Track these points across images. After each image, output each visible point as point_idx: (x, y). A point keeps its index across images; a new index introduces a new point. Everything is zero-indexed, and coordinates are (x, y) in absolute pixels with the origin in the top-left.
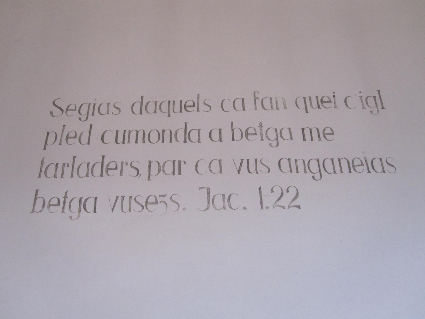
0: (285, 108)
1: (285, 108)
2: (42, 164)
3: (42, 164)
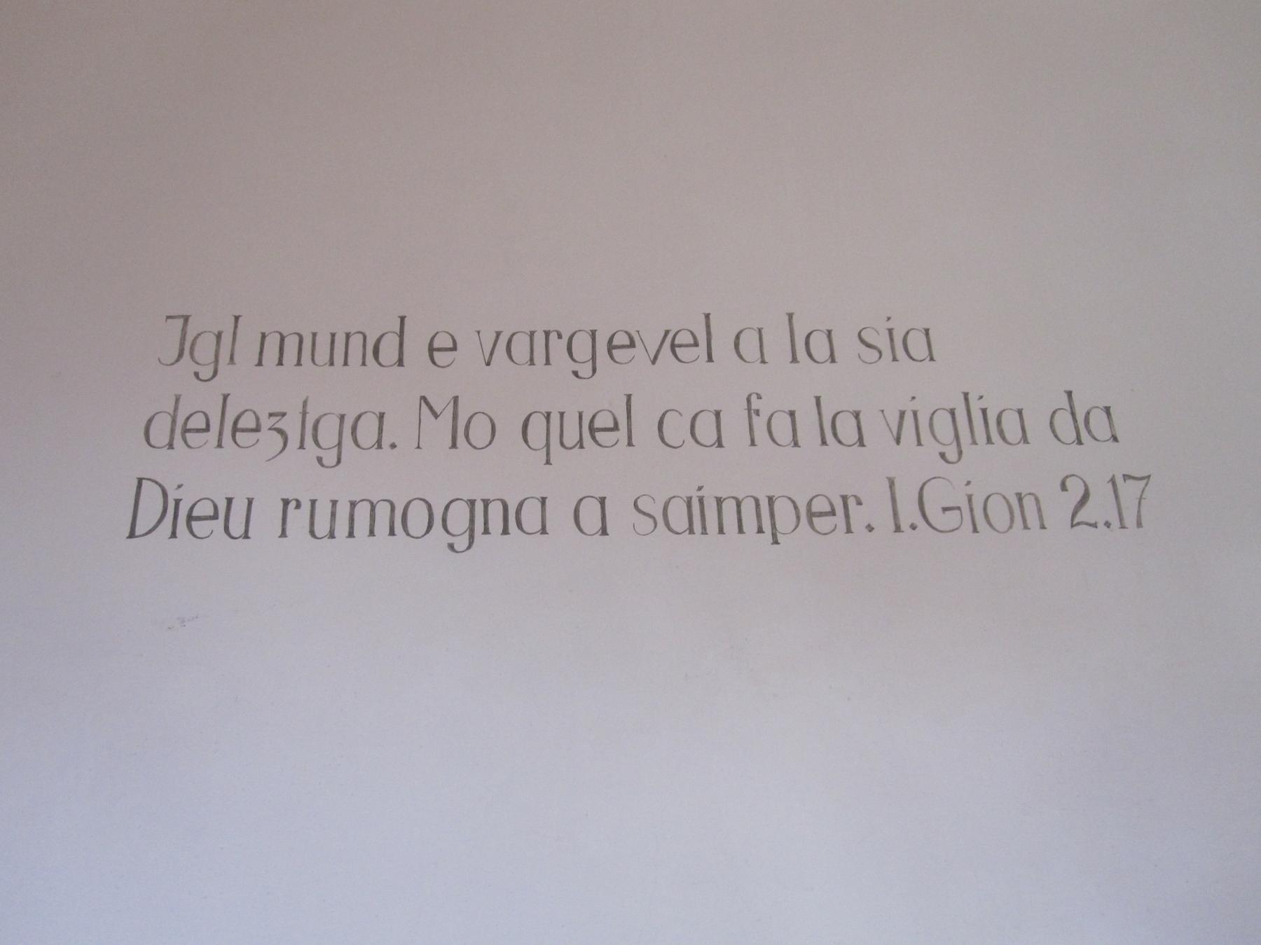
0: (1139, 524)
1: (1139, 524)
2: (304, 414)
3: (304, 414)
